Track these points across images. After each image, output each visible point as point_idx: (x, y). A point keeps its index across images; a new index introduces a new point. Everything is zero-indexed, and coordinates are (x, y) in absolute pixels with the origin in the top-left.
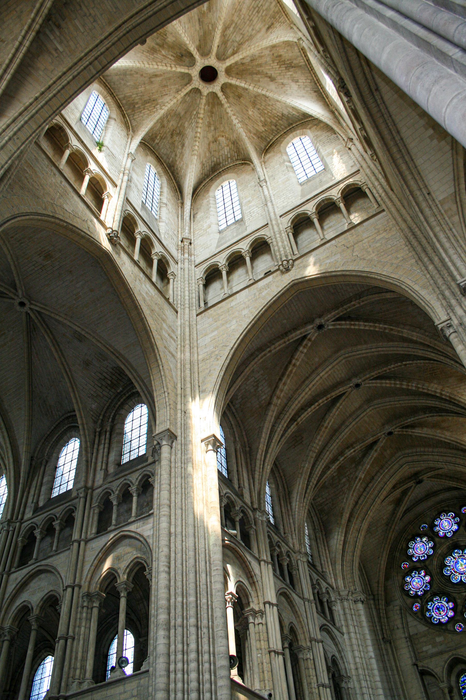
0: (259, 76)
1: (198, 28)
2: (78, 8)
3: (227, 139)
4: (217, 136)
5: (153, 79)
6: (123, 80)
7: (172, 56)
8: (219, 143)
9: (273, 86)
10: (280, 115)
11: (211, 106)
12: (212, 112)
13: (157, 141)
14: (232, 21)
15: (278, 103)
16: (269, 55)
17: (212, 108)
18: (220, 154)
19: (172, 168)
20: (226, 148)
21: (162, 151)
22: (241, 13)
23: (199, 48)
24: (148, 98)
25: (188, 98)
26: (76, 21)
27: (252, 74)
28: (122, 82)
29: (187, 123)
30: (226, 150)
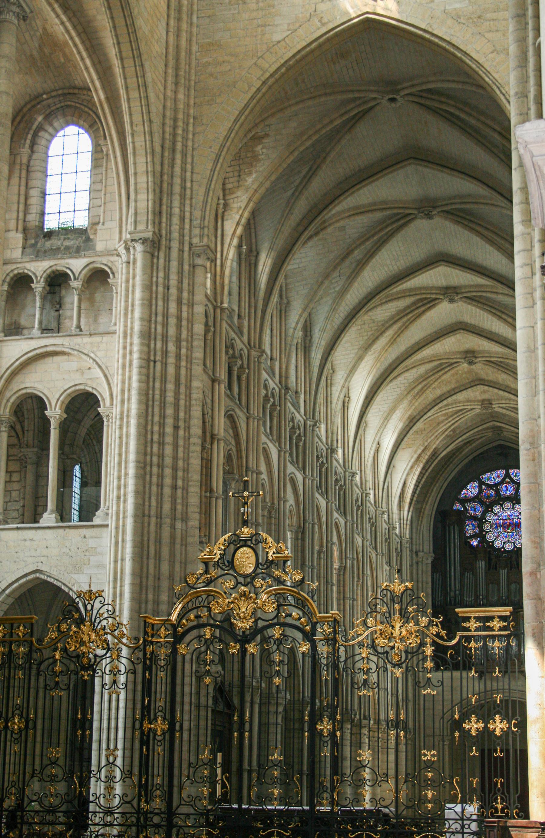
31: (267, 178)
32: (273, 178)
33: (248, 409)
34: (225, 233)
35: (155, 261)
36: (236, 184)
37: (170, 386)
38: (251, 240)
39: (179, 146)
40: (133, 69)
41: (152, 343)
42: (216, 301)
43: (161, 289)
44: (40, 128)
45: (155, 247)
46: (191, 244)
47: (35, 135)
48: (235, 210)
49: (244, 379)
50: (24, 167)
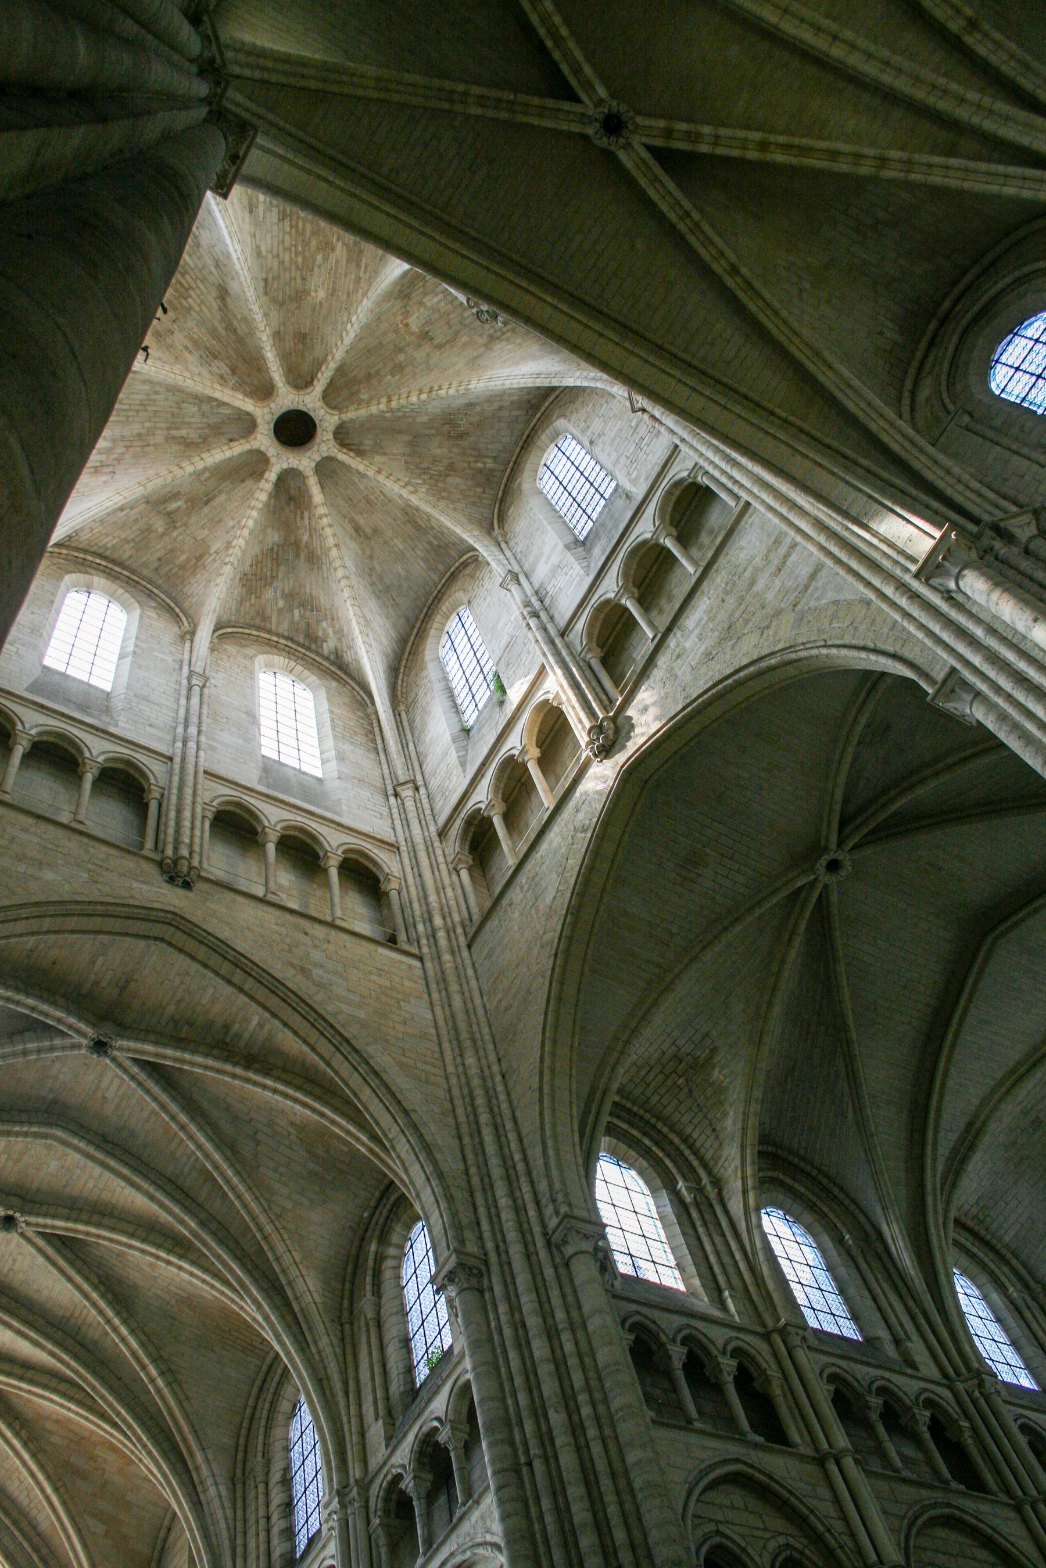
0: (235, 323)
1: (222, 498)
2: (183, 1004)
3: (407, 312)
4: (413, 338)
5: (369, 531)
6: (400, 587)
7: (302, 518)
8: (426, 323)
9: (233, 287)
10: (287, 223)
11: (355, 388)
12: (369, 376)
13: (490, 464)
14: (168, 439)
15: (263, 249)
16: (181, 330)
17: (360, 382)
18: (449, 307)
19: (533, 402)
20: (429, 304)
21: (507, 439)
22: (144, 431)
23: (258, 474)
24: (409, 525)
25: (366, 442)
26: (204, 1001)
27: (240, 341)
28: (405, 585)
29: (419, 420)
30: (431, 301)
31: (748, 1102)
32: (758, 1094)
33: (1009, 1492)
34: (735, 1218)
35: (487, 1295)
36: (716, 1144)
37: (575, 1491)
38: (859, 1222)
39: (484, 1118)
40: (346, 1063)
41: (516, 1431)
42: (763, 1324)
43: (507, 1332)
44: (380, 1259)
45: (480, 1274)
46: (545, 1234)
47: (377, 1273)
48: (733, 1177)
49: (970, 1441)
50: (372, 1323)
